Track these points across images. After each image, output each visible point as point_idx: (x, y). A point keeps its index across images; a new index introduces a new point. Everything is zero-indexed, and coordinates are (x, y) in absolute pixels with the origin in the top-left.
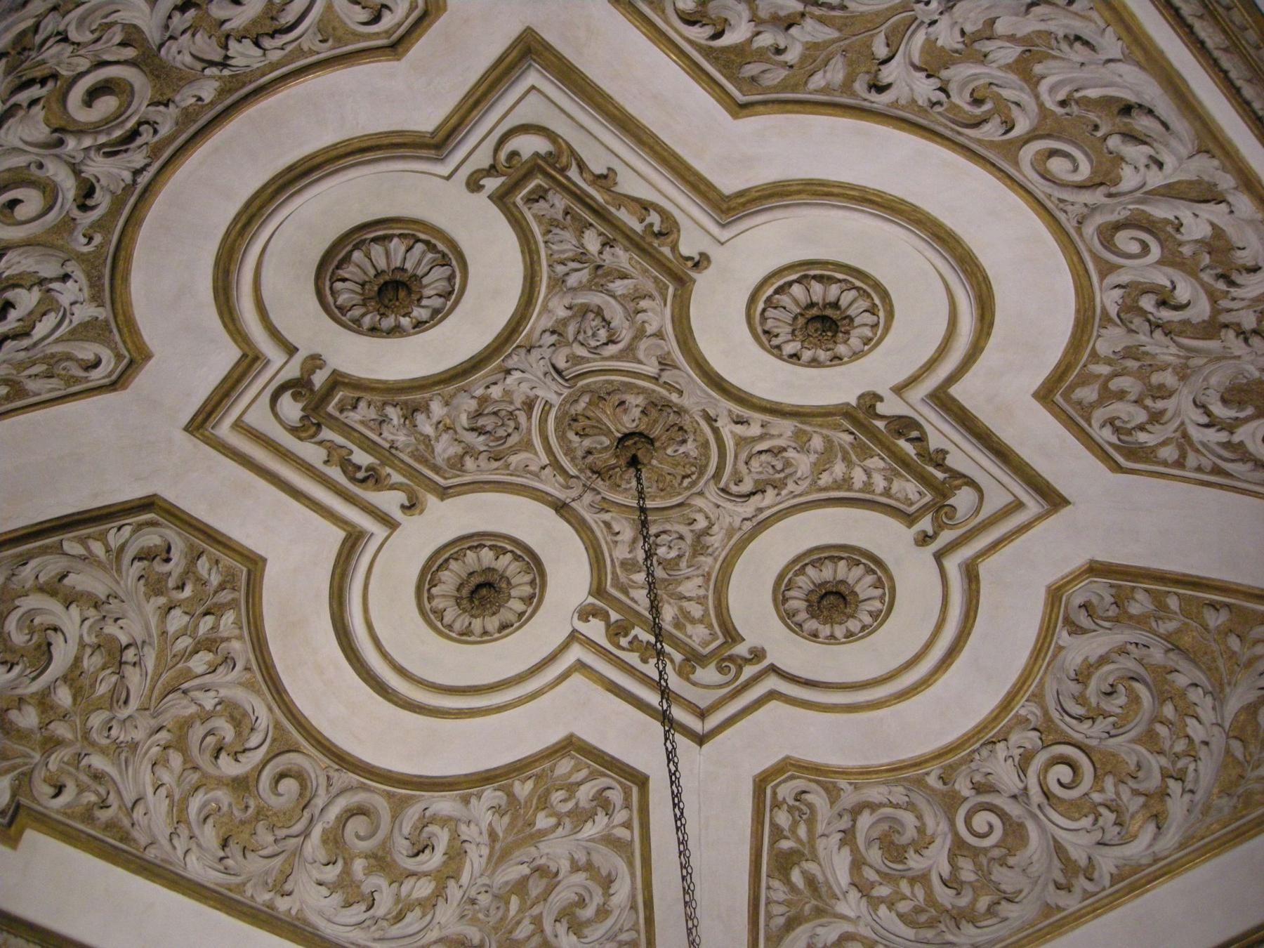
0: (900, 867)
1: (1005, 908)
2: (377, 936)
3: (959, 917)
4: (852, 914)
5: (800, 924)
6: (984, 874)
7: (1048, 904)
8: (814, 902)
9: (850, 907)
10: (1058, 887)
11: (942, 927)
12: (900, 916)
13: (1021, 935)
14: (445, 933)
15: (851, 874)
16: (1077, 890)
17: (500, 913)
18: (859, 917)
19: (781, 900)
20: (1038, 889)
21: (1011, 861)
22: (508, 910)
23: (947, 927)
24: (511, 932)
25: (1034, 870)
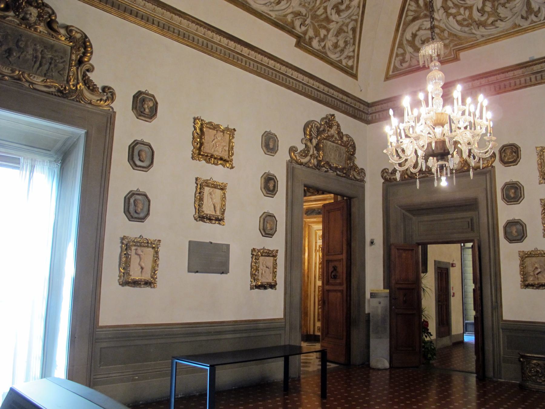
0: (463, 2)
1: (499, 24)
2: (271, 9)
3: (480, 24)
4: (439, 18)
5: (418, 20)
6: (495, 9)
7: (515, 24)
8: (425, 12)
9: (439, 16)
10: (522, 17)
11: (472, 27)
12: (457, 21)
13: (501, 34)
14: (294, 10)
15: (443, 3)
16: (529, 21)
17: (313, 5)
18: (441, 20)
19: (413, 10)
20: (514, 17)
21: (507, 5)
22: (316, 3)
23: (474, 27)
24: (316, 12)
25: (515, 10)
